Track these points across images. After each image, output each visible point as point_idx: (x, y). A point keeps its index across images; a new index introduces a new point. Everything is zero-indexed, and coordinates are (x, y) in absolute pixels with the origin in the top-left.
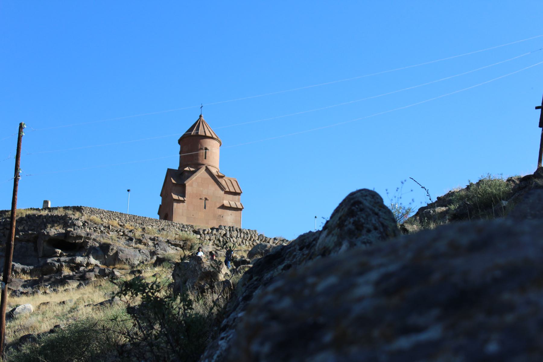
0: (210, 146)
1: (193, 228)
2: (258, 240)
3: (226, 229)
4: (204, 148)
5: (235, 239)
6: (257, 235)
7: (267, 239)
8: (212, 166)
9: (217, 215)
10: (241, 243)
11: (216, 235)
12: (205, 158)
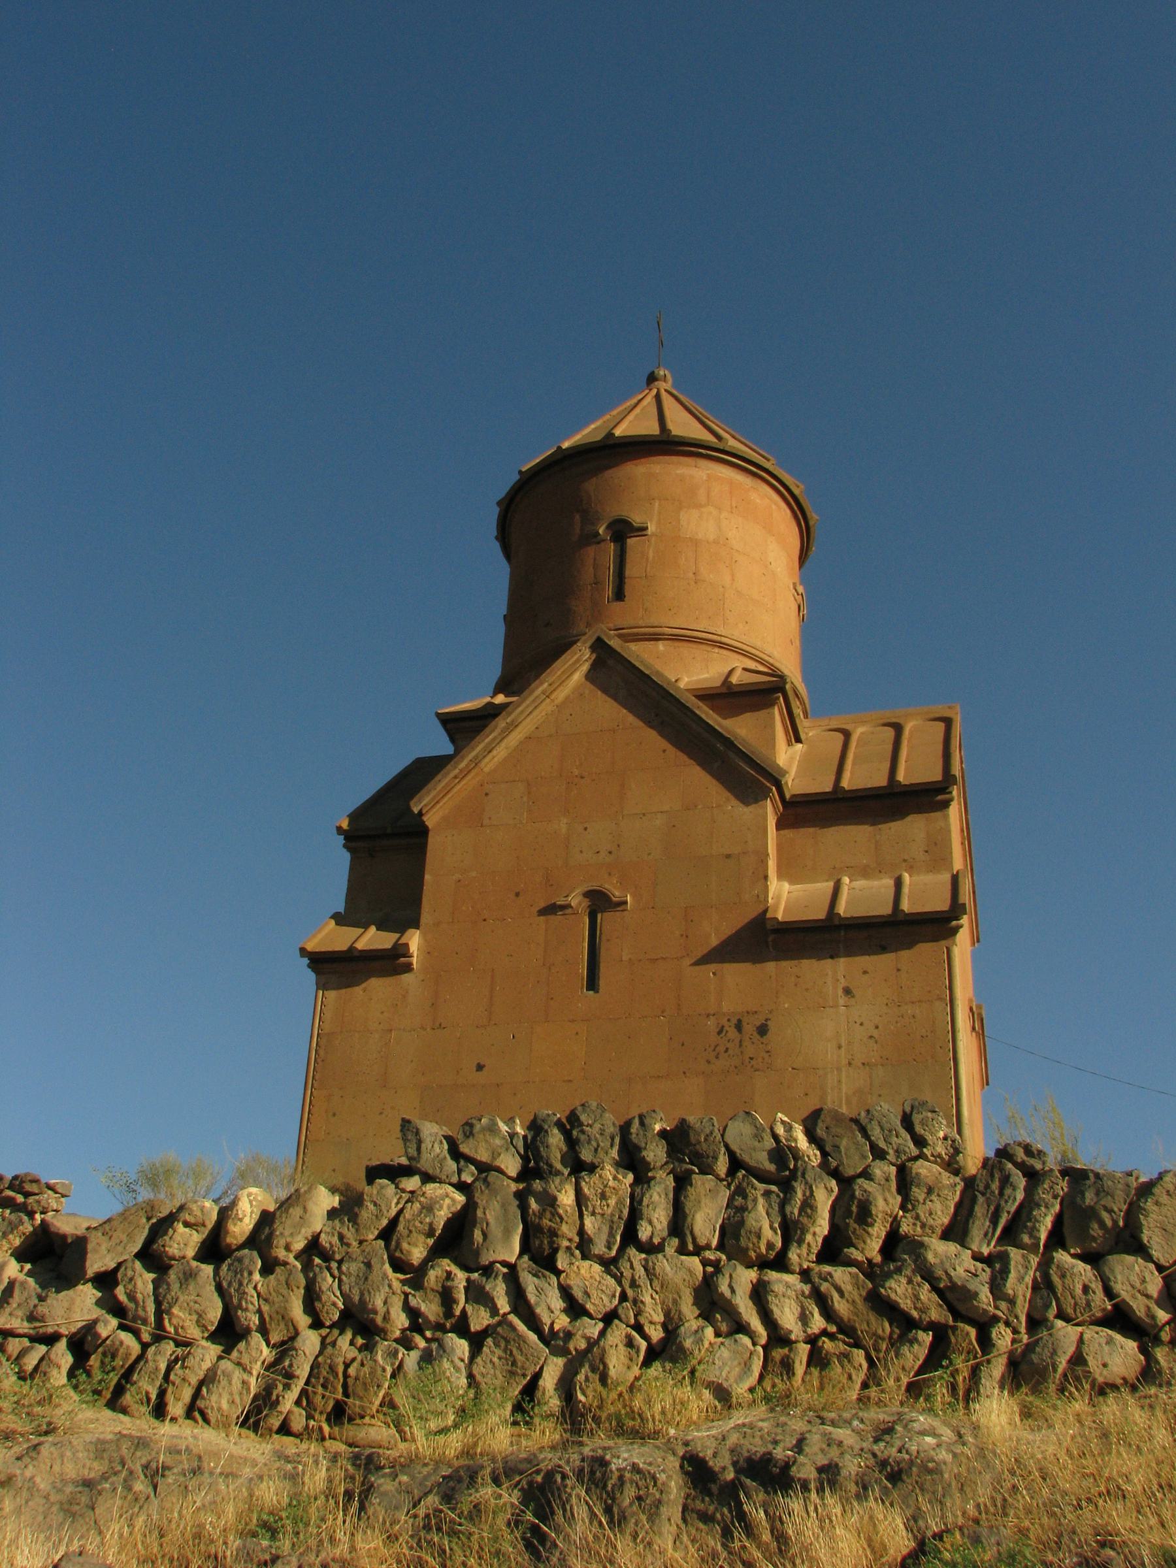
0: (657, 504)
1: (31, 1215)
2: (956, 1232)
3: (483, 1156)
4: (601, 531)
5: (597, 1268)
6: (952, 1165)
7: (1089, 1198)
8: (675, 638)
9: (711, 1023)
10: (688, 1309)
11: (327, 1257)
12: (619, 595)
